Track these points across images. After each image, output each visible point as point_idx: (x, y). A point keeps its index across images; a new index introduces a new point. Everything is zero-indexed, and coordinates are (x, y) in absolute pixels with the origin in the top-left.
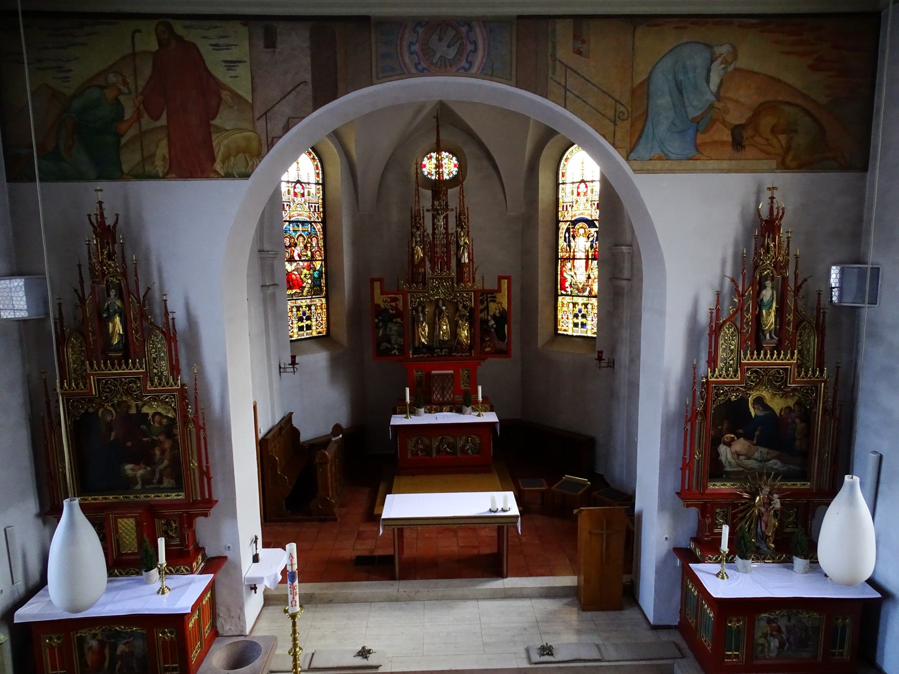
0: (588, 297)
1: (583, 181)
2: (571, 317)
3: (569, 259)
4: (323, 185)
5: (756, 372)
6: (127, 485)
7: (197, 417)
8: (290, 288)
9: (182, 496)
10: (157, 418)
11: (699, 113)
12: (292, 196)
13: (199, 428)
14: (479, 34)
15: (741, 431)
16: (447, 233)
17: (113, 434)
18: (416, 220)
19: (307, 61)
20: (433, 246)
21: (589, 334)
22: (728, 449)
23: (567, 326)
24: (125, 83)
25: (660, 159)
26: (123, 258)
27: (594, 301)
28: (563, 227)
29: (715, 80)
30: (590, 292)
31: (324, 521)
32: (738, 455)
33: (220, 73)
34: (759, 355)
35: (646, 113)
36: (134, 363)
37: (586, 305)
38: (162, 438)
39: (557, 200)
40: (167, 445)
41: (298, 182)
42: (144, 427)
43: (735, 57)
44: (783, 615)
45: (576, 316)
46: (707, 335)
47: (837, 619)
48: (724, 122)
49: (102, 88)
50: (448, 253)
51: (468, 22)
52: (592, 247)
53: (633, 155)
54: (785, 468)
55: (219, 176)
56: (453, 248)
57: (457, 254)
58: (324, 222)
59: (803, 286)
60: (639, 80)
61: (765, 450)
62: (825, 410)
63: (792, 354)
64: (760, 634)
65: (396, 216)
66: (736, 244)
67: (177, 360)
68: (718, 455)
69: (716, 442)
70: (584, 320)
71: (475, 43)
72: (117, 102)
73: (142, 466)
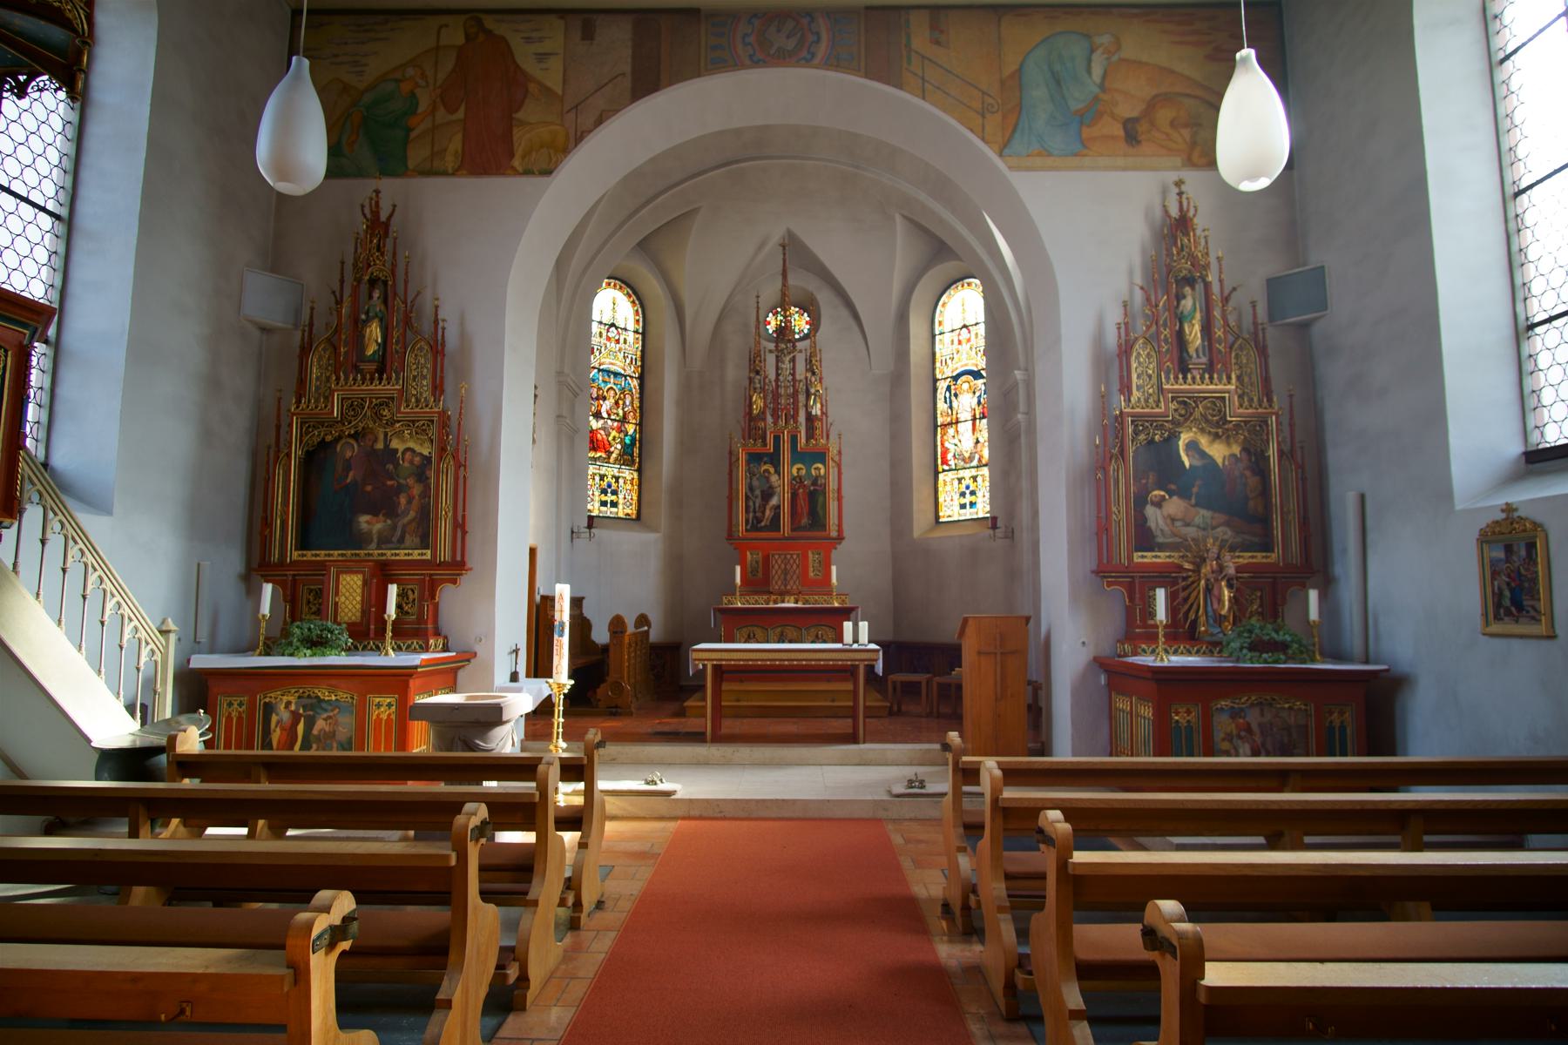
2: (956, 497)
3: (950, 424)
4: (643, 334)
5: (1184, 403)
6: (357, 540)
7: (457, 450)
8: (594, 449)
9: (428, 555)
10: (408, 455)
11: (1081, 106)
12: (603, 340)
13: (459, 465)
14: (822, 26)
15: (1173, 487)
16: (794, 379)
18: (754, 364)
19: (627, 53)
20: (776, 396)
21: (981, 515)
23: (951, 510)
24: (423, 76)
25: (1039, 154)
26: (394, 254)
27: (985, 471)
28: (942, 386)
29: (1097, 72)
31: (614, 714)
33: (528, 64)
34: (1185, 378)
35: (1020, 106)
36: (389, 379)
37: (975, 478)
38: (411, 481)
39: (934, 354)
40: (417, 490)
41: (613, 325)
42: (390, 467)
43: (1119, 48)
44: (1252, 705)
45: (963, 495)
46: (1113, 365)
47: (1331, 713)
48: (1113, 116)
49: (397, 81)
50: (796, 403)
51: (810, 13)
52: (979, 403)
53: (1006, 151)
54: (1239, 540)
55: (517, 173)
56: (802, 398)
57: (806, 406)
58: (641, 378)
59: (1234, 295)
60: (1007, 72)
62: (1281, 453)
63: (1229, 378)
64: (1222, 735)
65: (734, 372)
66: (1144, 252)
67: (442, 378)
68: (1145, 519)
69: (1141, 501)
70: (973, 498)
71: (818, 34)
72: (413, 95)
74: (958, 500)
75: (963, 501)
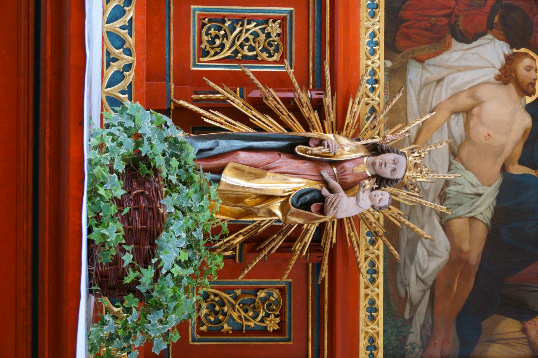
22: (491, 74)
32: (468, 112)
54: (415, 289)
61: (484, 208)
68: (468, 38)
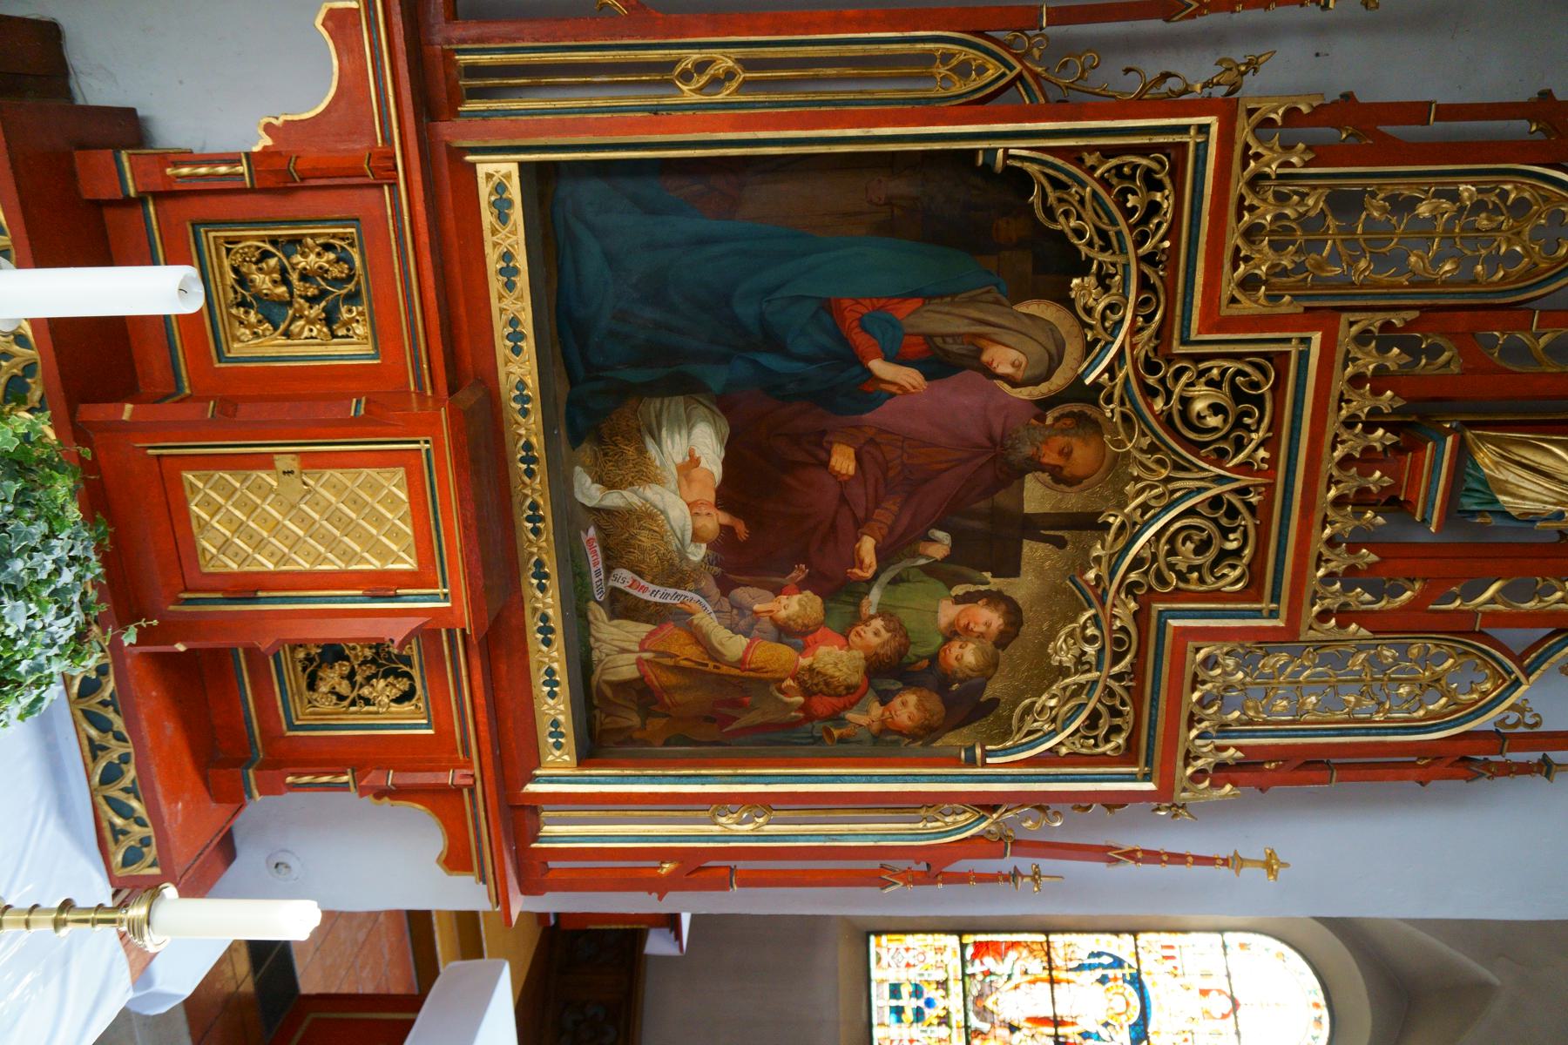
0: (967, 1027)
1: (1235, 1005)
2: (914, 975)
10: (988, 618)
17: (908, 377)
28: (1121, 946)
30: (978, 1033)
37: (944, 1020)
38: (874, 634)
39: (1185, 931)
40: (837, 659)
42: (940, 545)
70: (909, 1015)
73: (713, 521)
74: (906, 977)
75: (906, 990)
